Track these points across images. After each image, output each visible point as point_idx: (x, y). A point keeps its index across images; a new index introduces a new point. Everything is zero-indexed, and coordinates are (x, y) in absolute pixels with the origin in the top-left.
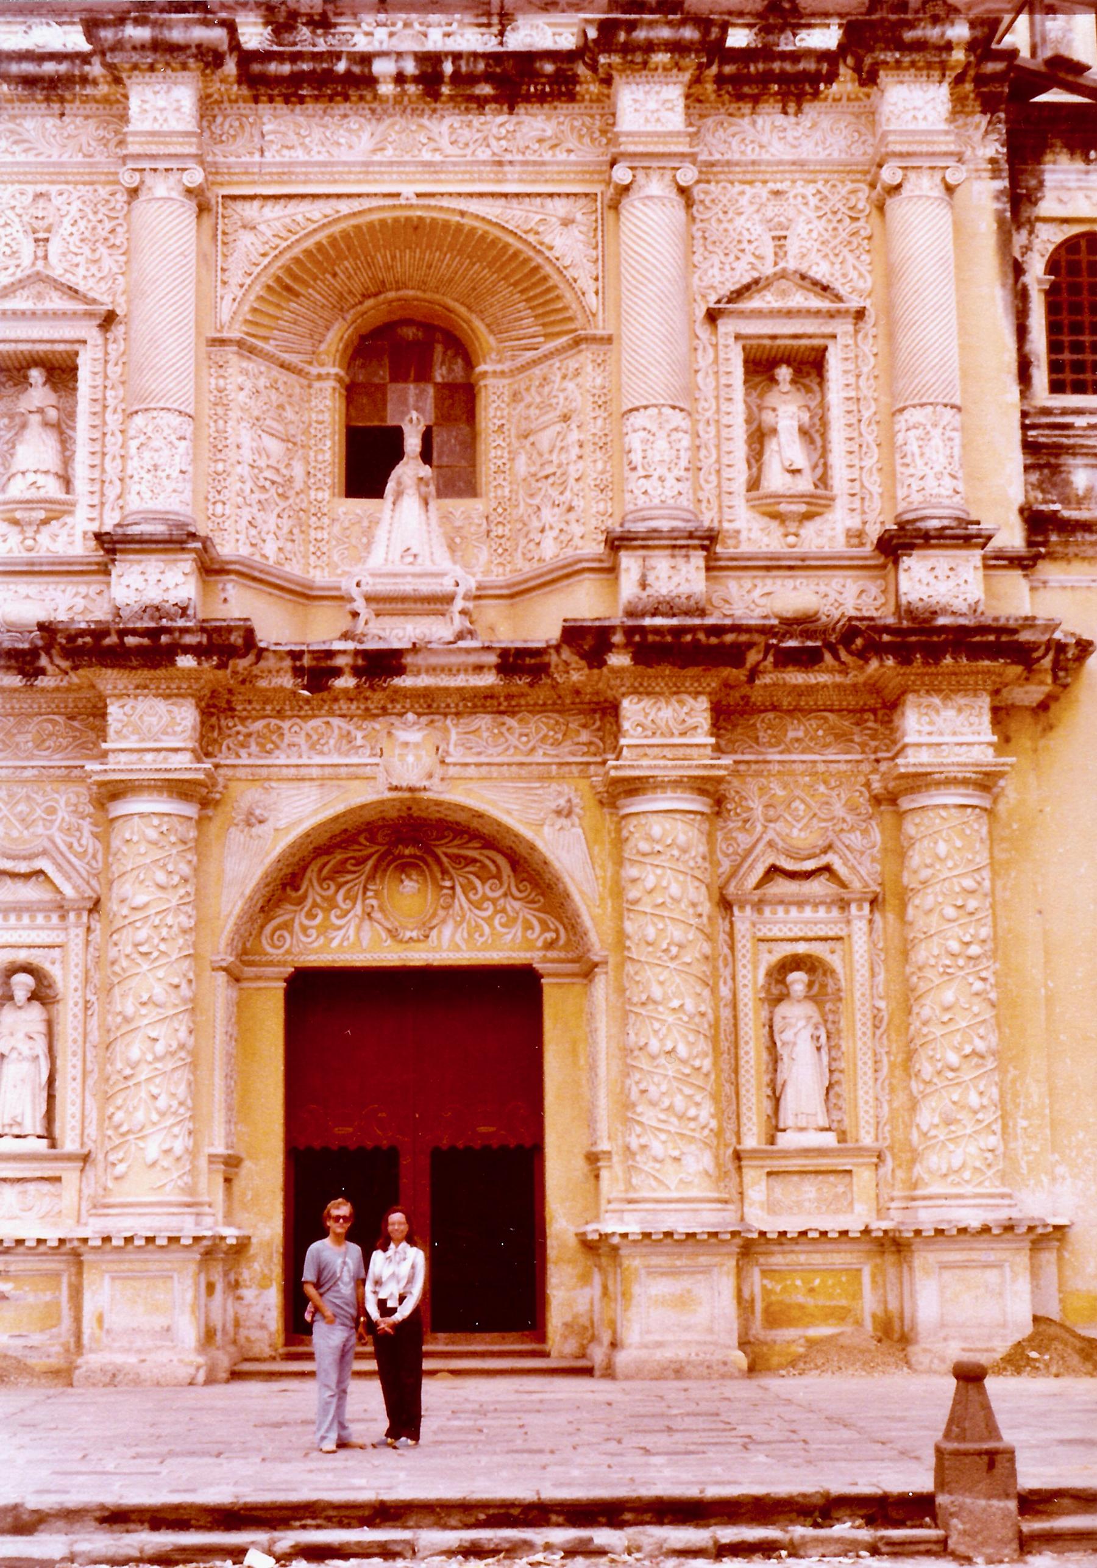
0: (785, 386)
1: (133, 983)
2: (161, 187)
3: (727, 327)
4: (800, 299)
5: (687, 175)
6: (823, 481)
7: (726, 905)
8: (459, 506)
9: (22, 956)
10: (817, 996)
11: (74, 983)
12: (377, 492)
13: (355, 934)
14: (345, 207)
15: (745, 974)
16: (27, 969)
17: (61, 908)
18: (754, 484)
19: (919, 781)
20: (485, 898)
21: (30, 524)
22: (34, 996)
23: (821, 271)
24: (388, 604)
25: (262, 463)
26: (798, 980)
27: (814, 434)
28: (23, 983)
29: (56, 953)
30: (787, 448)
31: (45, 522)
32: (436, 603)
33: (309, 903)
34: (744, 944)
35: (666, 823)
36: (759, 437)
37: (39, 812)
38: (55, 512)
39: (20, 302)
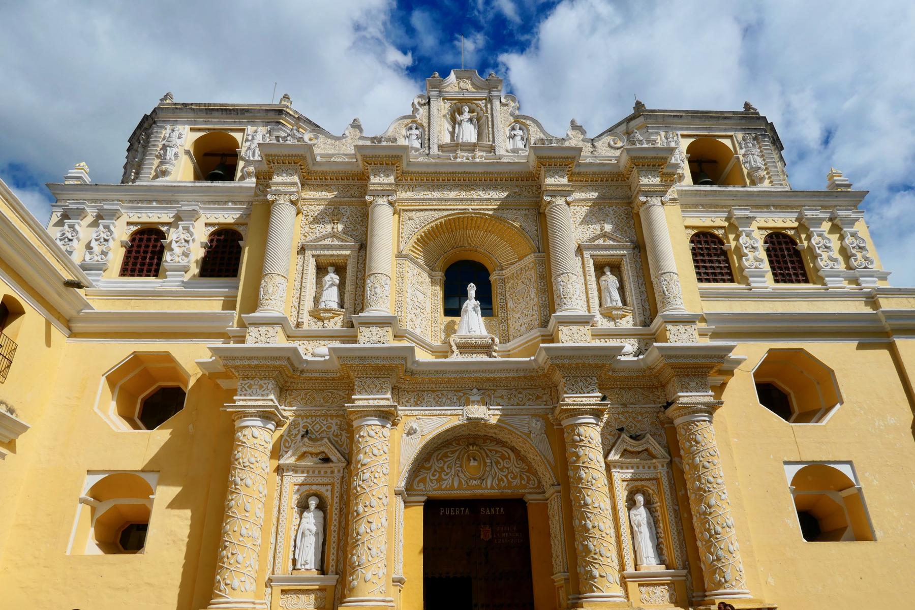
0: (609, 273)
1: (363, 497)
9: (314, 487)
11: (336, 500)
16: (316, 495)
20: (504, 467)
21: (326, 319)
24: (465, 348)
25: (416, 300)
29: (329, 487)
31: (333, 318)
33: (433, 470)
37: (324, 428)
39: (328, 242)
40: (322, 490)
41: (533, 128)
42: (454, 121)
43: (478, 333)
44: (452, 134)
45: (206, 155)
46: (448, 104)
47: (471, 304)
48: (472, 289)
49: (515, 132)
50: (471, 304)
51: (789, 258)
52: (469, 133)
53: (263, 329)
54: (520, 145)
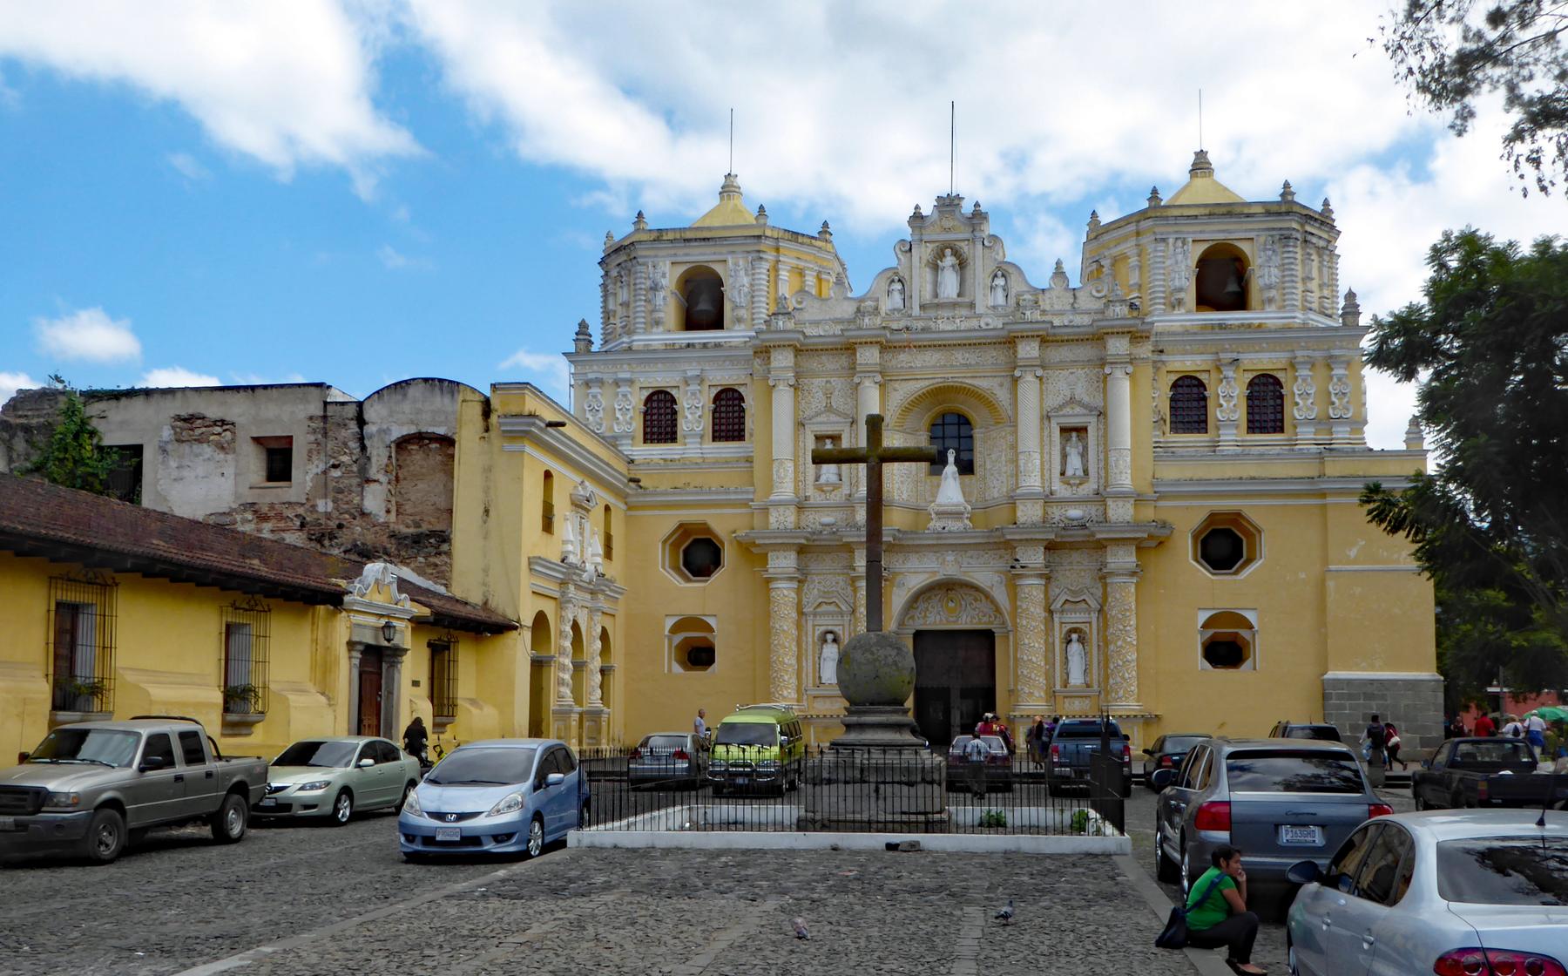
2: (867, 383)
3: (1054, 422)
4: (1078, 410)
5: (1039, 372)
6: (1086, 472)
7: (1051, 612)
8: (967, 478)
10: (1081, 640)
12: (940, 473)
13: (936, 618)
14: (927, 383)
15: (1057, 633)
17: (842, 614)
18: (1063, 474)
19: (1111, 574)
22: (835, 641)
23: (1086, 399)
24: (942, 514)
26: (1074, 636)
27: (1084, 455)
28: (830, 637)
30: (1075, 463)
32: (957, 515)
34: (1057, 625)
35: (1032, 588)
36: (1064, 456)
38: (835, 487)
40: (835, 629)
41: (1013, 278)
42: (936, 268)
43: (955, 501)
44: (936, 284)
45: (687, 281)
46: (931, 246)
47: (951, 469)
48: (951, 457)
49: (1000, 282)
50: (951, 469)
51: (1266, 405)
52: (950, 285)
53: (781, 509)
54: (1001, 300)
